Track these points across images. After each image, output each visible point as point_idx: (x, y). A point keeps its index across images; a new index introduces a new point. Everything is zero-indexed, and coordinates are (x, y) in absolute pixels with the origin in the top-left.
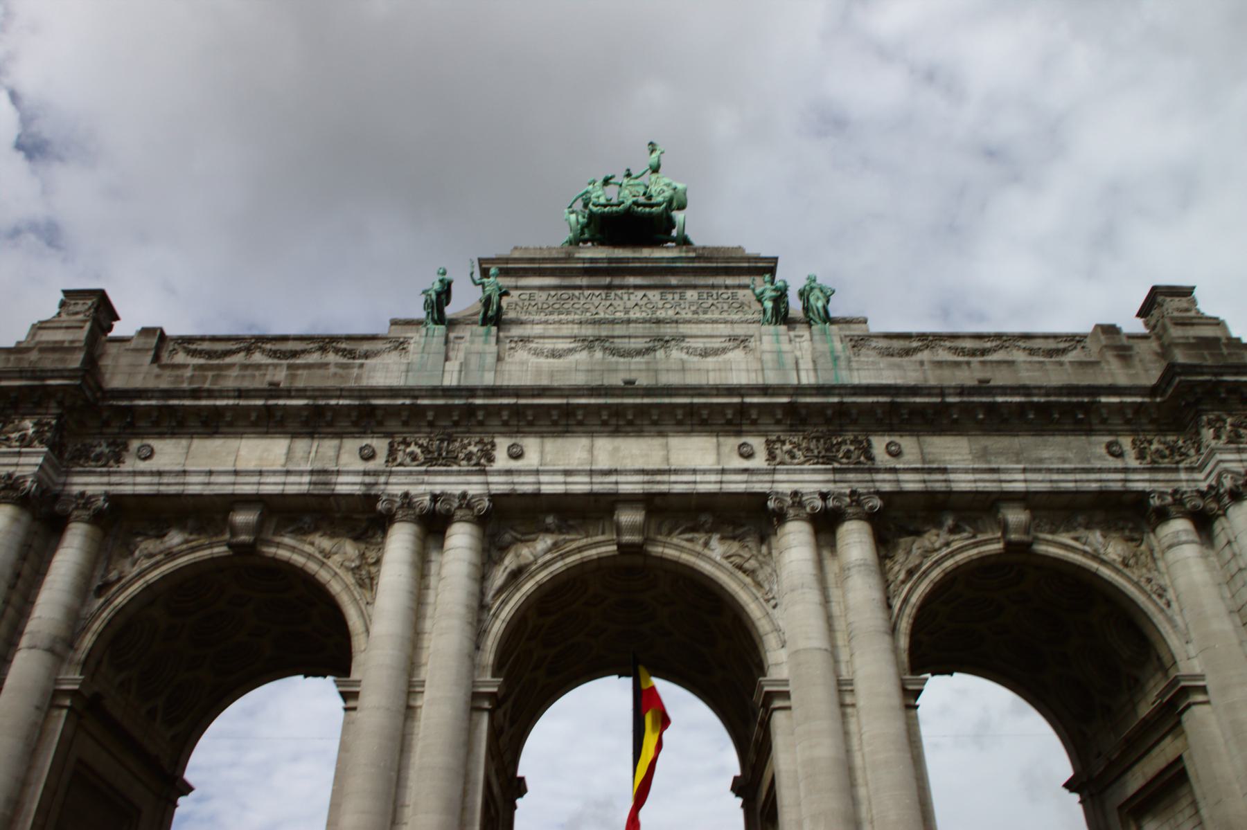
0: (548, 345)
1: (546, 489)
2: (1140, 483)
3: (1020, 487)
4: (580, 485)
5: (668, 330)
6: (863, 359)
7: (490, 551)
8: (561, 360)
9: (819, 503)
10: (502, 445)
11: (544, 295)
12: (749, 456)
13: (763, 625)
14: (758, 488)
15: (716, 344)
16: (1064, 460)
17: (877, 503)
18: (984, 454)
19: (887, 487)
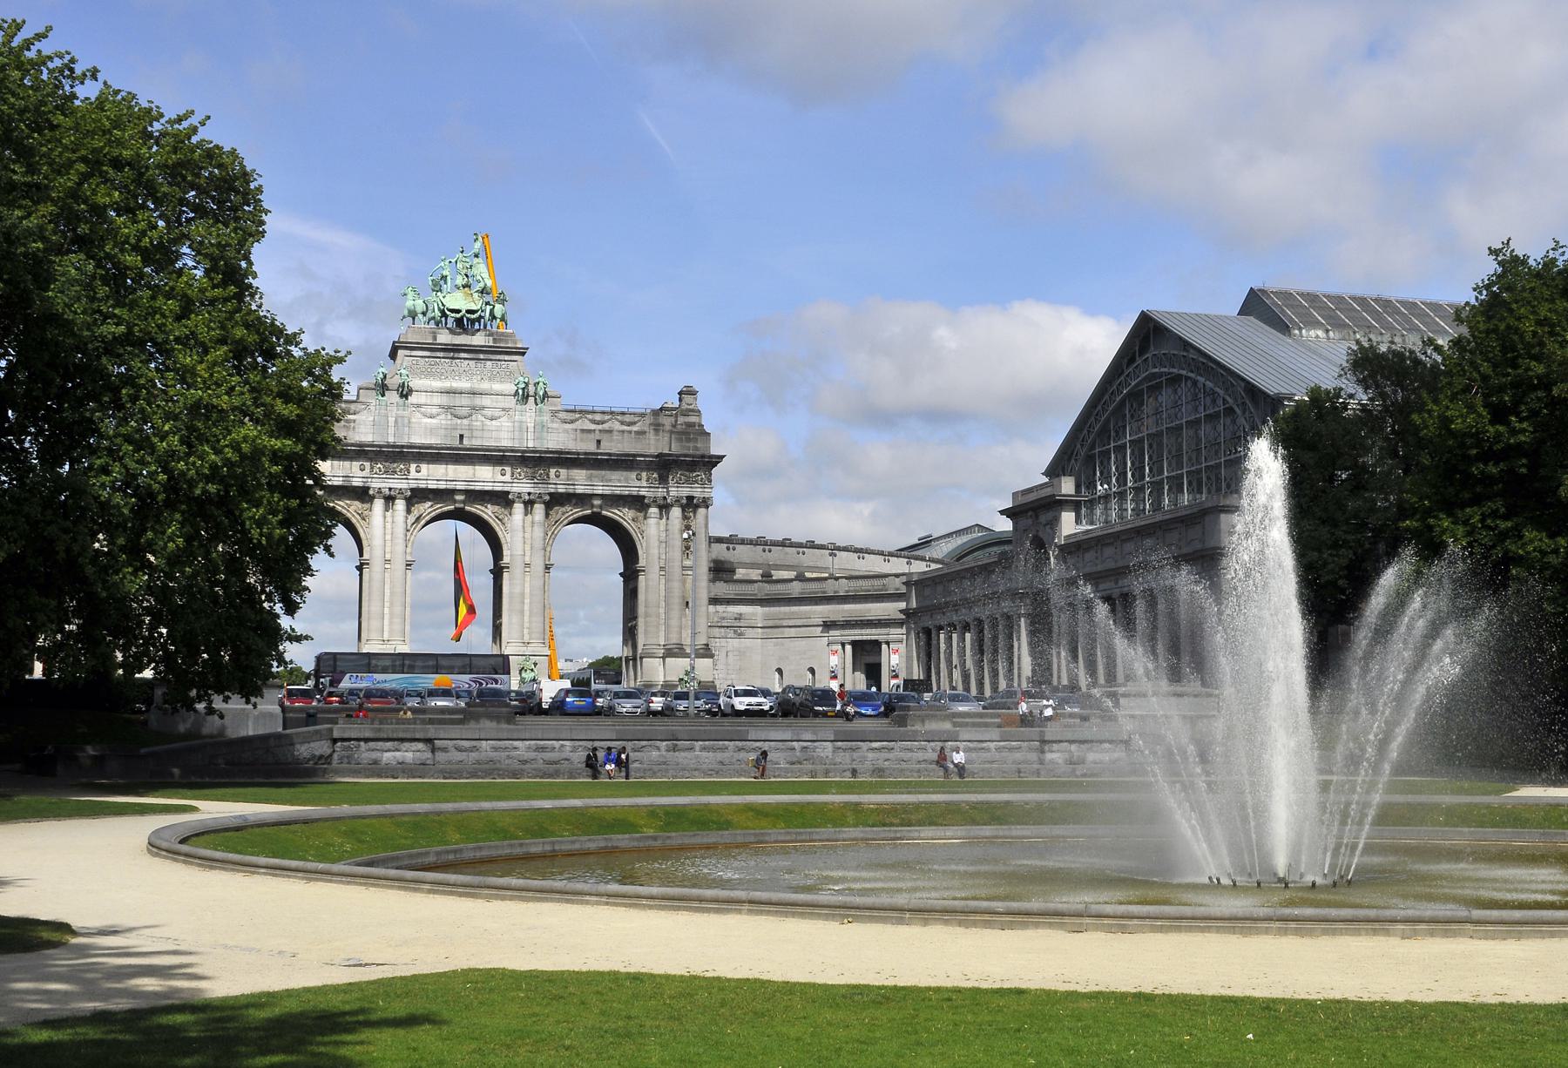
0: (430, 410)
1: (430, 487)
2: (643, 492)
3: (600, 492)
4: (442, 485)
5: (478, 401)
6: (555, 425)
7: (409, 511)
8: (434, 421)
9: (527, 498)
10: (413, 467)
11: (422, 360)
12: (503, 475)
13: (503, 541)
14: (506, 489)
15: (497, 413)
16: (619, 481)
17: (547, 498)
18: (590, 478)
19: (552, 491)
